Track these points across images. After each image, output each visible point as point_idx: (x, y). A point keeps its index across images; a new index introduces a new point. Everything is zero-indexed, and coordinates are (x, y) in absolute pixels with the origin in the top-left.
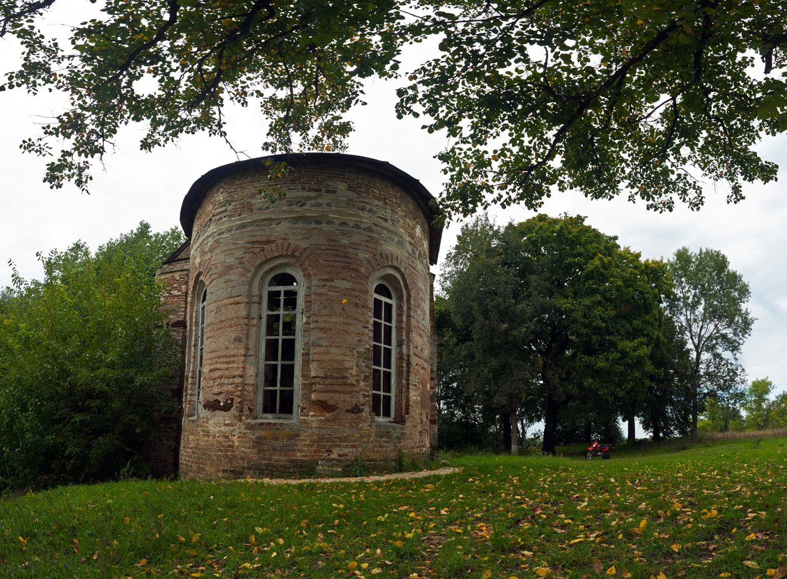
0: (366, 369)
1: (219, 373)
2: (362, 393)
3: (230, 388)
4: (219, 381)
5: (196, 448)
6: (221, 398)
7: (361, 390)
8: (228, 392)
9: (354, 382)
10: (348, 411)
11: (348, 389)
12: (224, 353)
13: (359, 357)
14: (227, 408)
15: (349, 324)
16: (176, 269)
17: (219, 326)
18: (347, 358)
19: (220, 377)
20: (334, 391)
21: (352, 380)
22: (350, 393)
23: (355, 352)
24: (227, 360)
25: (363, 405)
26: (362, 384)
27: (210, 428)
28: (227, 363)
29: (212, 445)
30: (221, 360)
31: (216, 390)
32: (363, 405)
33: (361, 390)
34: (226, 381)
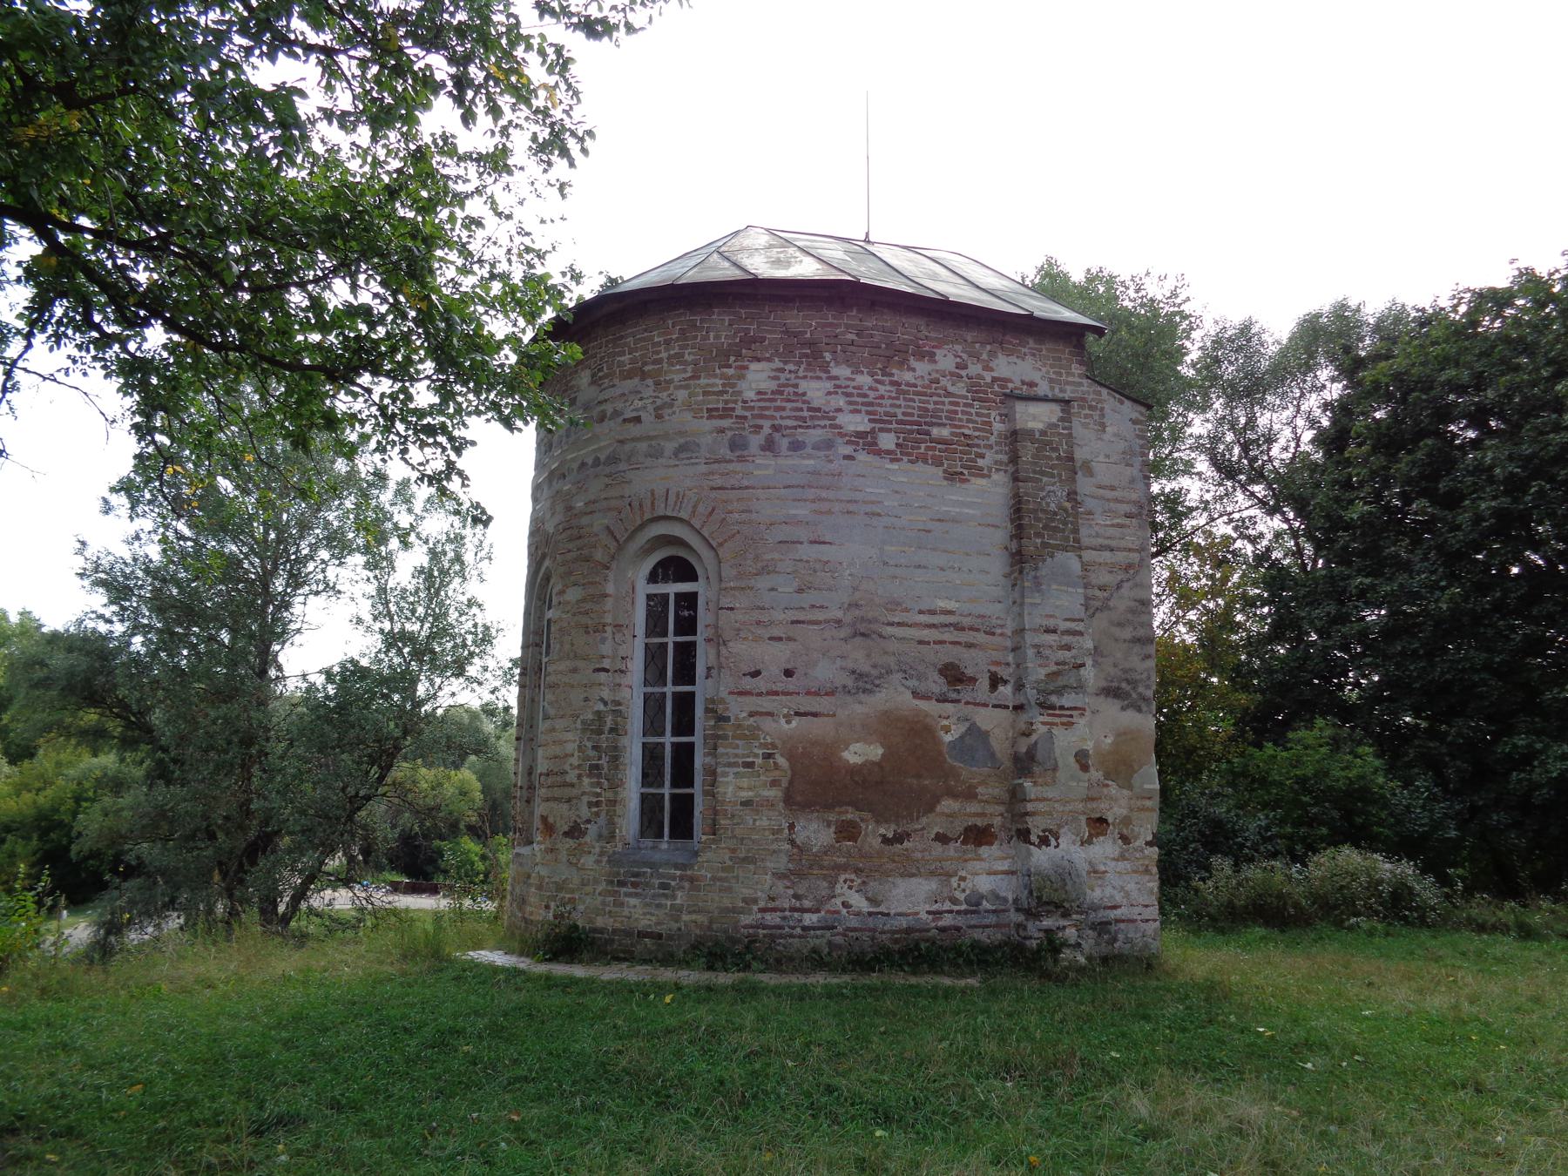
0: (592, 753)
2: (585, 799)
7: (584, 793)
9: (575, 780)
10: (566, 834)
11: (568, 792)
13: (584, 730)
15: (575, 670)
18: (570, 736)
20: (555, 799)
21: (571, 777)
22: (569, 800)
23: (579, 725)
25: (588, 821)
26: (586, 781)
32: (588, 821)
33: (584, 793)
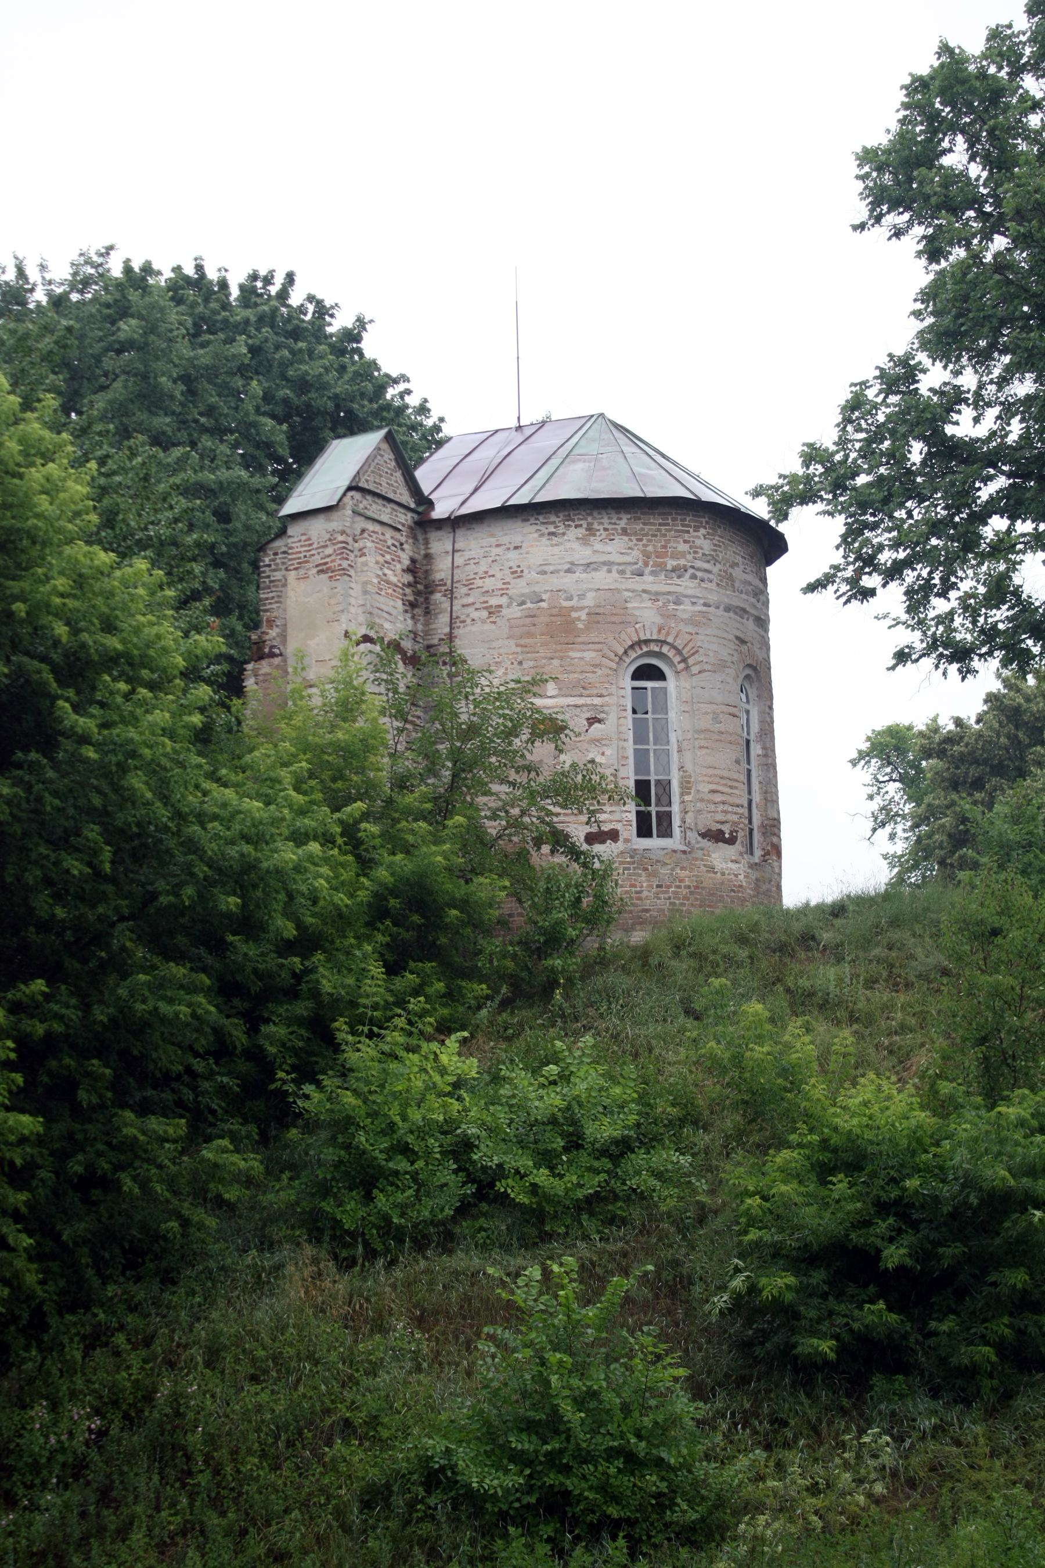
1: (718, 798)
3: (735, 818)
4: (721, 807)
5: (697, 887)
6: (726, 829)
8: (734, 823)
12: (725, 773)
14: (731, 841)
16: (369, 514)
17: (717, 737)
19: (724, 803)
24: (730, 783)
27: (715, 863)
28: (731, 787)
29: (722, 883)
30: (724, 782)
31: (720, 817)
34: (730, 809)
